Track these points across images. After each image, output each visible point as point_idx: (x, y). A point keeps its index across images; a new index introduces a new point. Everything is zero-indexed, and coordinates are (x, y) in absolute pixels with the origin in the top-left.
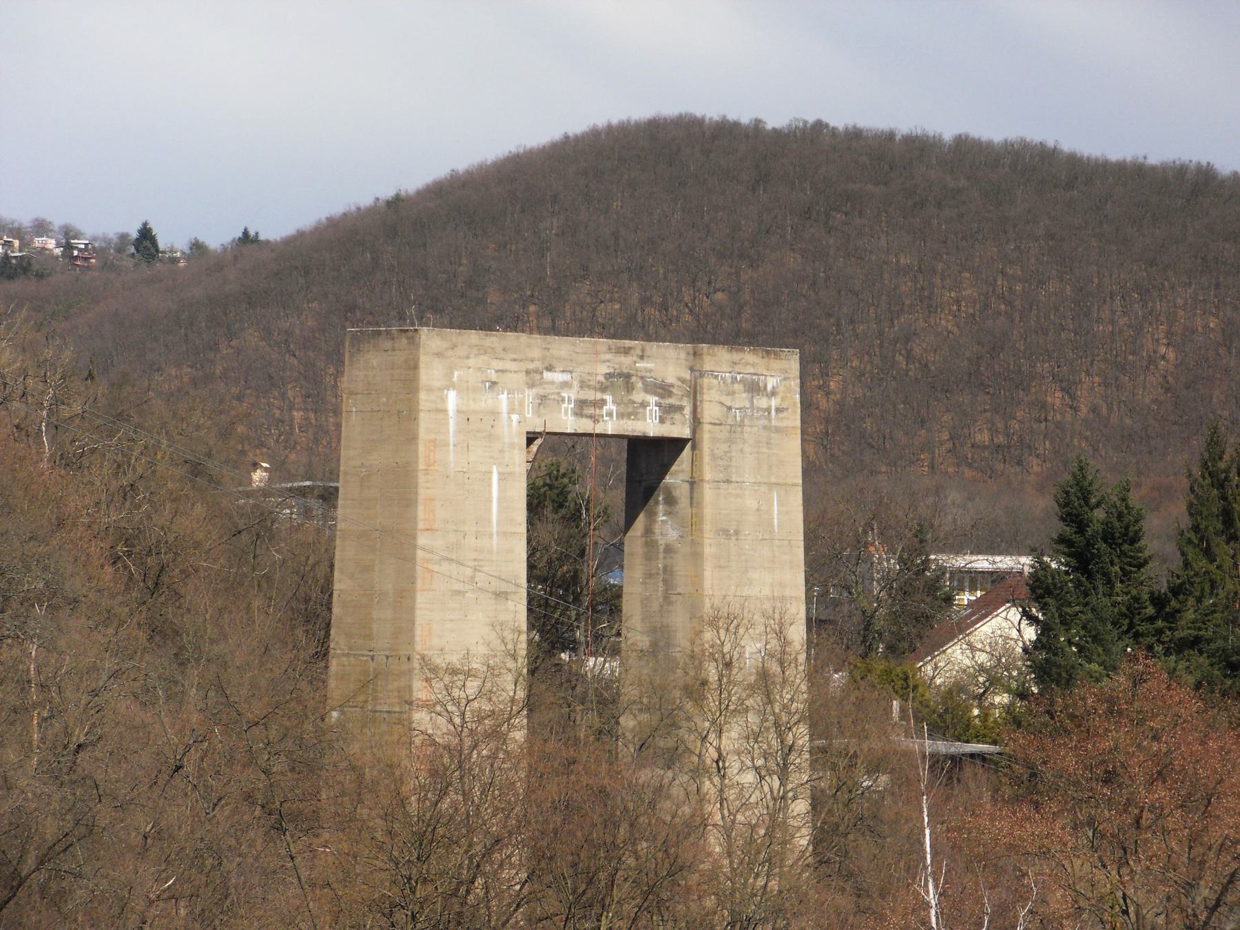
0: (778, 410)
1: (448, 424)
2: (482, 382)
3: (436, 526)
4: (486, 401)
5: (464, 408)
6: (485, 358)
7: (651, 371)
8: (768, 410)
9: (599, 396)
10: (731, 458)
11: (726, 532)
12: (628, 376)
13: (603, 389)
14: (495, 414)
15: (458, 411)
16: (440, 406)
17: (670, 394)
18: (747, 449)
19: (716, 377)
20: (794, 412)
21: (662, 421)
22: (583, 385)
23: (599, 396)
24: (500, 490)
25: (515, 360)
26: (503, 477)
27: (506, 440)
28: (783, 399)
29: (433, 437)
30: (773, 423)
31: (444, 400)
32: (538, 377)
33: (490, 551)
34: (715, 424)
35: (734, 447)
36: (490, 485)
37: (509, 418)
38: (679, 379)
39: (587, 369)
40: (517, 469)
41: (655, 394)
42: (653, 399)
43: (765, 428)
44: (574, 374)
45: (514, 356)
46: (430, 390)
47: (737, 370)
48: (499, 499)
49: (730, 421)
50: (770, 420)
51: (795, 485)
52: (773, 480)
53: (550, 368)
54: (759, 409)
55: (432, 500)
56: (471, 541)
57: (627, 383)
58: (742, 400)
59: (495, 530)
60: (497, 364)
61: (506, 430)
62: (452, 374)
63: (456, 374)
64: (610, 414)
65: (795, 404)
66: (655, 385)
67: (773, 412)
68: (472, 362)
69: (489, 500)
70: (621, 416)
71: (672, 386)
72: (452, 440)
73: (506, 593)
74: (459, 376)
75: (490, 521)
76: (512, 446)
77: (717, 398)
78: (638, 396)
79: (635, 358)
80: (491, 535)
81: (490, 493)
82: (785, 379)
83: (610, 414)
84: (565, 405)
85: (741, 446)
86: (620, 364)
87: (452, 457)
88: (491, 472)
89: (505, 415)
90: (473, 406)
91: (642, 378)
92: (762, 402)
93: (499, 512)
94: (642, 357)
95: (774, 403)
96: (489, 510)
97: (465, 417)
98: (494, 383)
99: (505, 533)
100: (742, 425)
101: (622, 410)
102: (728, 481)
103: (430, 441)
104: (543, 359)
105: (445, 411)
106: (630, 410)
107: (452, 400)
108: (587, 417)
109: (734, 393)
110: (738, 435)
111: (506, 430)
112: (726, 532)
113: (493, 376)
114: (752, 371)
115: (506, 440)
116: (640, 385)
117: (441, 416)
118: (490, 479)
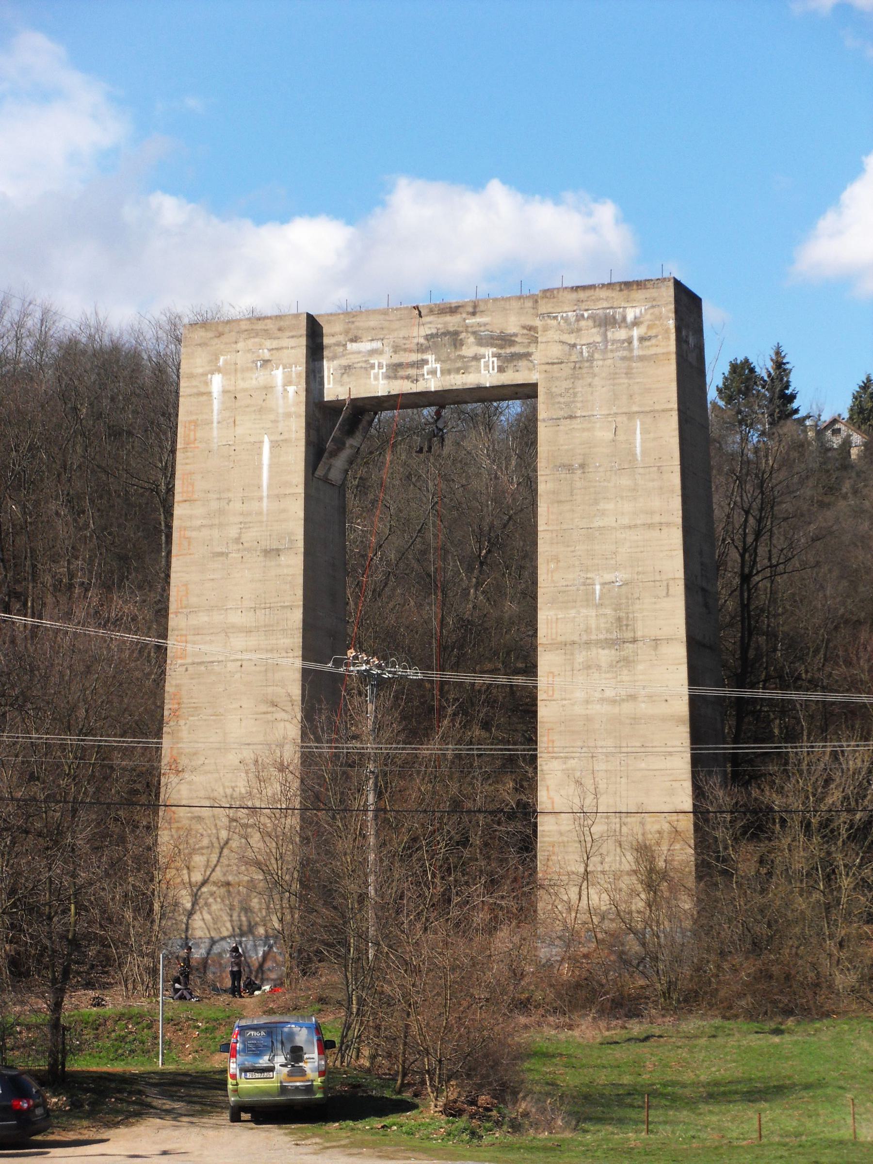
0: (642, 339)
1: (212, 405)
2: (253, 362)
3: (196, 496)
4: (259, 378)
5: (232, 388)
6: (256, 340)
7: (485, 325)
8: (630, 341)
9: (420, 356)
10: (575, 394)
11: (569, 468)
12: (456, 333)
13: (421, 349)
14: (268, 389)
15: (225, 392)
16: (203, 389)
17: (512, 343)
18: (596, 381)
19: (555, 318)
20: (668, 338)
21: (501, 370)
22: (396, 349)
23: (420, 356)
24: (272, 455)
25: (293, 337)
26: (275, 445)
27: (281, 411)
28: (649, 327)
29: (194, 417)
30: (636, 353)
31: (207, 383)
32: (341, 349)
33: (260, 513)
34: (553, 364)
35: (579, 383)
36: (260, 454)
37: (285, 390)
38: (524, 327)
39: (402, 333)
40: (293, 436)
41: (492, 345)
42: (489, 351)
43: (623, 359)
44: (385, 341)
45: (291, 334)
46: (191, 376)
47: (584, 306)
48: (270, 466)
49: (574, 358)
50: (631, 350)
51: (671, 410)
52: (635, 409)
53: (354, 340)
54: (614, 342)
55: (190, 473)
56: (237, 506)
57: (455, 340)
58: (593, 335)
59: (265, 494)
60: (269, 344)
61: (281, 402)
62: (217, 359)
63: (222, 359)
64: (433, 372)
65: (667, 331)
66: (492, 337)
67: (636, 343)
68: (240, 345)
69: (260, 467)
70: (446, 372)
71: (516, 335)
72: (215, 418)
73: (278, 550)
74: (225, 361)
75: (259, 487)
76: (288, 415)
77: (556, 338)
78: (470, 349)
79: (464, 315)
80: (260, 499)
81: (260, 460)
82: (653, 307)
83: (433, 372)
84: (376, 370)
85: (590, 380)
86: (445, 323)
87: (215, 433)
88: (262, 442)
89: (280, 388)
90: (241, 384)
91: (474, 333)
92: (621, 334)
93: (271, 477)
94: (474, 314)
95: (636, 333)
96: (260, 477)
97: (231, 395)
98: (266, 362)
99: (278, 496)
100: (591, 359)
101: (447, 366)
102: (571, 417)
103: (190, 422)
104: (347, 332)
105: (209, 394)
106: (459, 364)
107: (217, 383)
108: (402, 378)
109: (579, 330)
110: (584, 371)
111: (281, 402)
112: (569, 468)
113: (266, 355)
114: (605, 305)
115: (281, 411)
116: (472, 339)
117: (204, 398)
118: (260, 448)
